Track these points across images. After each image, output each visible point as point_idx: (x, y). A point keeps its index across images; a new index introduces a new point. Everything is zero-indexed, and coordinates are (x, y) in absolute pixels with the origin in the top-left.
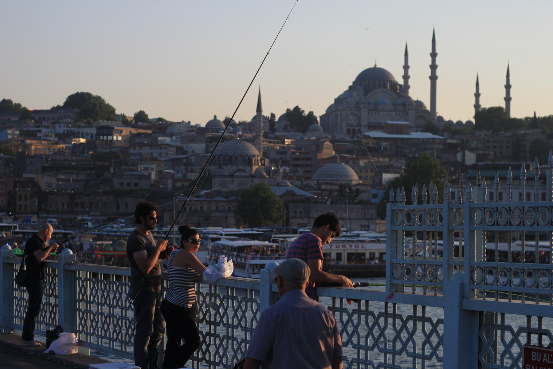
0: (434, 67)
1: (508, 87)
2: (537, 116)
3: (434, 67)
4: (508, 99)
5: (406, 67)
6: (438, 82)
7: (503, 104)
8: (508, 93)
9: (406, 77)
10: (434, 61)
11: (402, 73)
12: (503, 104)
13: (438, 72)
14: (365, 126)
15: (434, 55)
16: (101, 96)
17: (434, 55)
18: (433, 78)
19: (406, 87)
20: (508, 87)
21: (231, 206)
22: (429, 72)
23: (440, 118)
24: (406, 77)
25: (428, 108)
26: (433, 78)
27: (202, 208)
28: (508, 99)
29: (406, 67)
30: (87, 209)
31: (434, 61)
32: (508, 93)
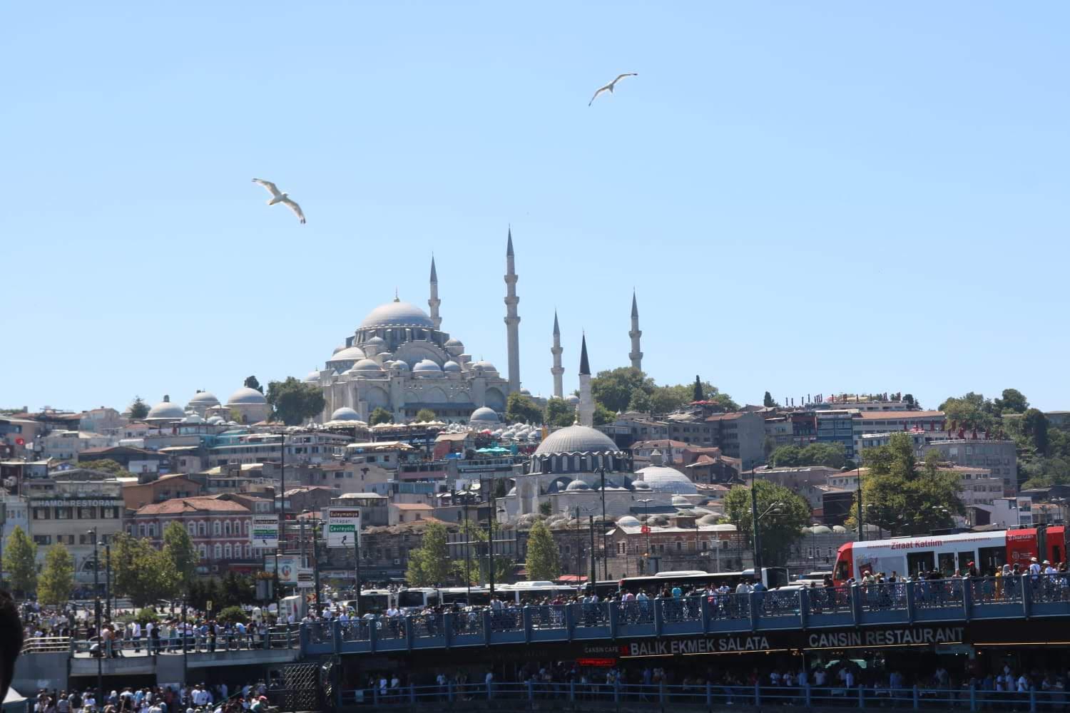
0: (512, 301)
1: (635, 335)
3: (512, 301)
4: (636, 356)
7: (629, 364)
8: (636, 345)
9: (437, 318)
10: (512, 290)
12: (629, 364)
13: (521, 310)
14: (400, 409)
15: (511, 279)
17: (511, 279)
18: (512, 321)
20: (635, 335)
21: (728, 541)
25: (504, 374)
26: (512, 321)
27: (679, 544)
28: (636, 356)
30: (397, 562)
31: (512, 290)
32: (636, 345)
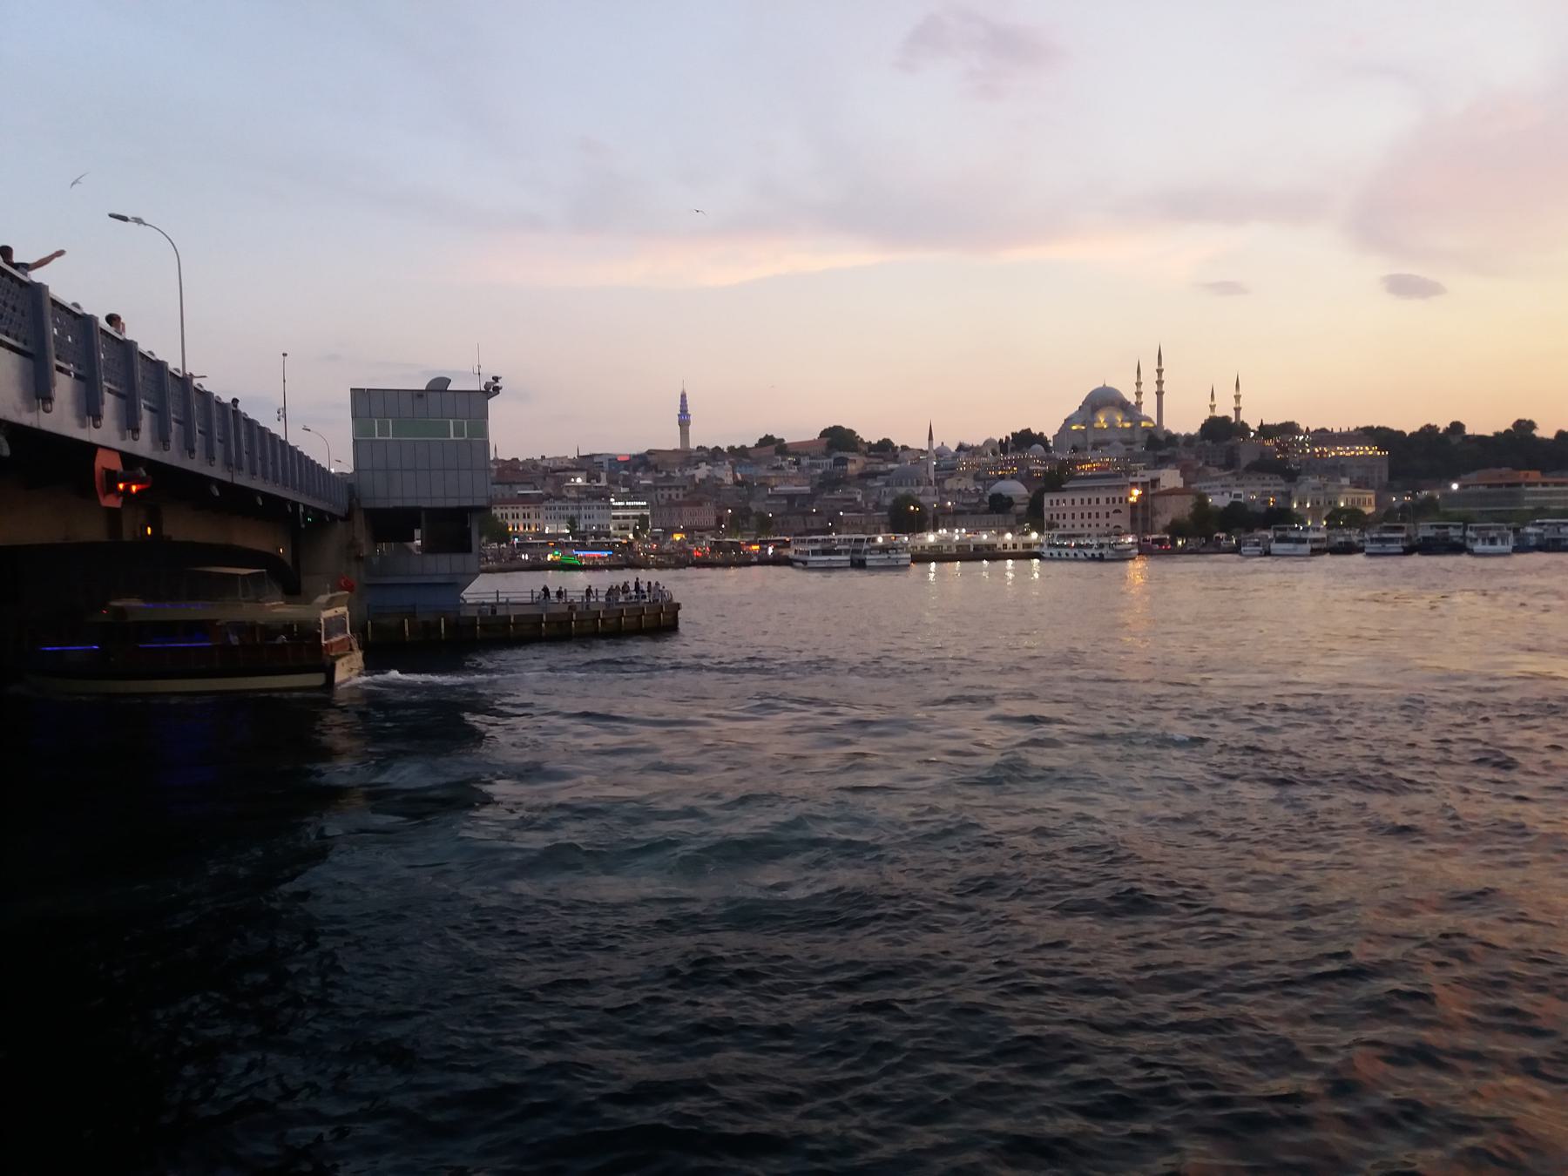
0: (1160, 383)
2: (1264, 423)
3: (1160, 383)
5: (1139, 384)
6: (1164, 396)
9: (1139, 394)
11: (1135, 389)
16: (854, 429)
17: (1160, 372)
19: (1139, 404)
22: (1155, 388)
23: (1168, 433)
24: (1139, 394)
26: (1160, 394)
28: (1237, 410)
29: (1139, 384)
